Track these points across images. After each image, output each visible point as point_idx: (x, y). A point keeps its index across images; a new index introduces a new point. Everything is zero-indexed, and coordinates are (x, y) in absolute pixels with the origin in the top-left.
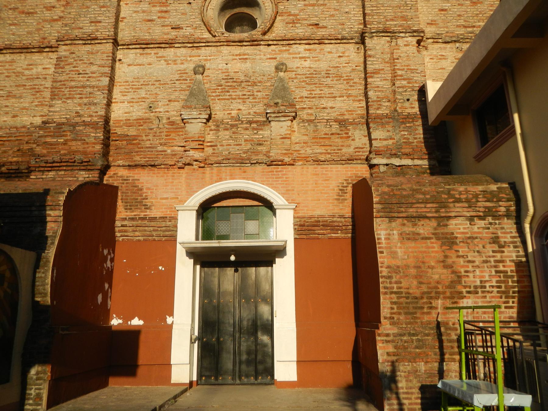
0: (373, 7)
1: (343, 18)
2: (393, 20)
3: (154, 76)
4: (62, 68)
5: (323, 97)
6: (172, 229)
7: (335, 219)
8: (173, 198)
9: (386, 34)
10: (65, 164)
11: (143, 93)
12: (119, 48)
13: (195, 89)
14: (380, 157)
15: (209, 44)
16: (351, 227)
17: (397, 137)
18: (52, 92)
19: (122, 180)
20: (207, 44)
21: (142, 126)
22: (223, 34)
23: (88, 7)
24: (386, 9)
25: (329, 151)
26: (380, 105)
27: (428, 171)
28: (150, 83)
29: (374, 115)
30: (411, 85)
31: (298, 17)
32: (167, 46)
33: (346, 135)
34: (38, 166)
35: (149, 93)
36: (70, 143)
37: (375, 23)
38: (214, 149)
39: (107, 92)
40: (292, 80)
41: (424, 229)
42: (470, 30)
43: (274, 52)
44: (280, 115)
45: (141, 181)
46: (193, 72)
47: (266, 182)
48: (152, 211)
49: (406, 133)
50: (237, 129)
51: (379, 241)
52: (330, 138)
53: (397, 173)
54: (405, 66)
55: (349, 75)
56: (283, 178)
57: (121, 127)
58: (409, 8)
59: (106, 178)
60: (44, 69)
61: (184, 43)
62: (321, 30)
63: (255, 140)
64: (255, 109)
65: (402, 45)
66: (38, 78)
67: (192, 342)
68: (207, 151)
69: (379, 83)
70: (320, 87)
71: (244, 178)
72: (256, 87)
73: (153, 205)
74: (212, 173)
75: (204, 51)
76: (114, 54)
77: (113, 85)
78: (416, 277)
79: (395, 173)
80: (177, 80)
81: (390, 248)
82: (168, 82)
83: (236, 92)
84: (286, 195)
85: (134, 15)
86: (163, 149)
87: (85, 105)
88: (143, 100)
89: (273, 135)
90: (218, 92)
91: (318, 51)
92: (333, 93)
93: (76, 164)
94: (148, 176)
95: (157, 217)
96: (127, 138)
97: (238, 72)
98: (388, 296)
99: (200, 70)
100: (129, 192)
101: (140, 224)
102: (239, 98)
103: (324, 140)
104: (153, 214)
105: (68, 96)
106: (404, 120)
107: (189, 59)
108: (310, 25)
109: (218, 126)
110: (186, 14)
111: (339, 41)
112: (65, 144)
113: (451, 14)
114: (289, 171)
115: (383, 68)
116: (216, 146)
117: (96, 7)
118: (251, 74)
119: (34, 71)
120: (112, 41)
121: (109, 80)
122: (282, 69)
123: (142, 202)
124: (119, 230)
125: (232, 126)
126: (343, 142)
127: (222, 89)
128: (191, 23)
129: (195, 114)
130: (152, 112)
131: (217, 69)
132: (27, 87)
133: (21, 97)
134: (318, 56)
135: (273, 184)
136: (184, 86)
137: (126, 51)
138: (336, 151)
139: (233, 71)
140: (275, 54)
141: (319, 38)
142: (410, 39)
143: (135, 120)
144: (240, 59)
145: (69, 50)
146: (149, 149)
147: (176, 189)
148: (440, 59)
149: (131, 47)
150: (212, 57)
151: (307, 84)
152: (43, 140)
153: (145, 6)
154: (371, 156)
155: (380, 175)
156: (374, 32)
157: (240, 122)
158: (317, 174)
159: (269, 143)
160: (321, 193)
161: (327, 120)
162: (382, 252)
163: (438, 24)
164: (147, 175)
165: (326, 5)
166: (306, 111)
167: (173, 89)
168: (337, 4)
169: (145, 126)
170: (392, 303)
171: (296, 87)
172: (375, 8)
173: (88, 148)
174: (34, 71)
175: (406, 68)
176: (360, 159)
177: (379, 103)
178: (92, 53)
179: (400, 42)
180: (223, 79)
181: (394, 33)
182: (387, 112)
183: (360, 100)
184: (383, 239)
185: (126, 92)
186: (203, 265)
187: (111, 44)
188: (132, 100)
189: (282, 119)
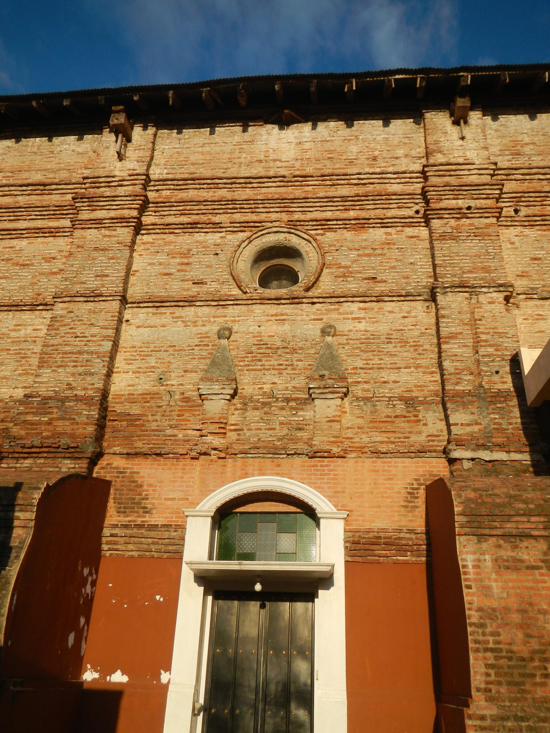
0: (445, 256)
1: (407, 270)
2: (471, 272)
3: (167, 341)
4: (56, 329)
5: (383, 368)
6: (177, 542)
7: (402, 535)
8: (183, 499)
9: (464, 290)
10: (46, 450)
11: (152, 361)
12: (127, 306)
13: (218, 356)
14: (463, 449)
15: (238, 302)
16: (425, 547)
17: (485, 422)
18: (40, 358)
19: (117, 472)
20: (236, 302)
21: (148, 402)
22: (256, 290)
23: (94, 259)
24: (463, 259)
25: (392, 439)
26: (460, 379)
27: (531, 469)
28: (162, 349)
29: (452, 392)
31: (350, 269)
32: (187, 304)
33: (415, 419)
34: (12, 451)
35: (160, 361)
36: (55, 423)
37: (449, 276)
38: (239, 435)
39: (108, 359)
40: (343, 346)
41: (529, 554)
43: (319, 312)
44: (327, 390)
45: (141, 474)
46: (216, 336)
47: (308, 481)
48: (153, 516)
49: (497, 417)
50: (270, 408)
51: (465, 570)
52: (393, 422)
53: (487, 471)
54: (490, 328)
55: (417, 340)
56: (329, 474)
57: (122, 403)
58: (492, 257)
59: (96, 469)
60: (34, 330)
61: (207, 301)
63: (293, 423)
64: (294, 383)
65: (485, 302)
66: (25, 341)
67: (195, 715)
68: (230, 437)
69: (457, 350)
70: (379, 355)
71: (277, 474)
72: (296, 355)
73: (155, 508)
74: (235, 466)
75: (232, 311)
76: (120, 313)
77: (117, 351)
78: (521, 626)
79: (484, 472)
80: (196, 346)
81: (481, 580)
83: (270, 361)
84: (334, 499)
85: (148, 268)
86: (173, 433)
87: (80, 374)
88: (153, 370)
89: (317, 417)
90: (248, 361)
91: (376, 310)
92: (396, 363)
93: (59, 450)
94: (151, 468)
95: (158, 525)
96: (128, 418)
97: (274, 336)
98: (480, 655)
100: (125, 489)
101: (135, 533)
102: (274, 369)
103: (386, 424)
104: (153, 519)
105: (59, 363)
106: (494, 400)
107: (212, 320)
108: (366, 279)
109: (245, 404)
110: (211, 267)
111: (402, 298)
112: (49, 423)
113: (547, 263)
114: (338, 466)
115: (461, 331)
116: (242, 430)
117: (104, 258)
118: (290, 338)
119: (22, 333)
120: (119, 298)
121: (112, 345)
122: (330, 332)
123: (140, 503)
124: (106, 541)
125: (264, 404)
126: (411, 427)
127: (252, 357)
128: (217, 277)
129: (216, 388)
130: (162, 386)
131: (247, 332)
132: (11, 352)
134: (375, 316)
135: (317, 483)
136: (205, 353)
137: (135, 310)
138: (402, 440)
139: (267, 334)
140: (322, 314)
141: (377, 295)
142: (495, 295)
143: (140, 394)
144: (276, 320)
145: (67, 308)
146: (155, 433)
147: (187, 486)
148: (537, 319)
149: (142, 305)
150: (242, 318)
151: (362, 351)
152: (22, 418)
153: (162, 258)
154: (450, 447)
155: (464, 473)
156: (447, 287)
157: (275, 399)
158: (376, 471)
159: (311, 427)
160: (383, 497)
161: (390, 398)
162: (469, 587)
163: (531, 276)
164: (149, 466)
165: (385, 255)
166: (360, 386)
167: (191, 357)
168: (399, 254)
169: (152, 403)
170: (487, 666)
171: (348, 356)
172: (448, 258)
173: (78, 429)
174: (22, 333)
175: (491, 331)
176: (435, 451)
177: (458, 376)
178: (94, 312)
179: (482, 298)
180: (254, 345)
181: (473, 288)
182: (469, 388)
183: (432, 373)
184: (470, 567)
185: (132, 360)
186: (217, 596)
187: (118, 302)
188: (139, 370)
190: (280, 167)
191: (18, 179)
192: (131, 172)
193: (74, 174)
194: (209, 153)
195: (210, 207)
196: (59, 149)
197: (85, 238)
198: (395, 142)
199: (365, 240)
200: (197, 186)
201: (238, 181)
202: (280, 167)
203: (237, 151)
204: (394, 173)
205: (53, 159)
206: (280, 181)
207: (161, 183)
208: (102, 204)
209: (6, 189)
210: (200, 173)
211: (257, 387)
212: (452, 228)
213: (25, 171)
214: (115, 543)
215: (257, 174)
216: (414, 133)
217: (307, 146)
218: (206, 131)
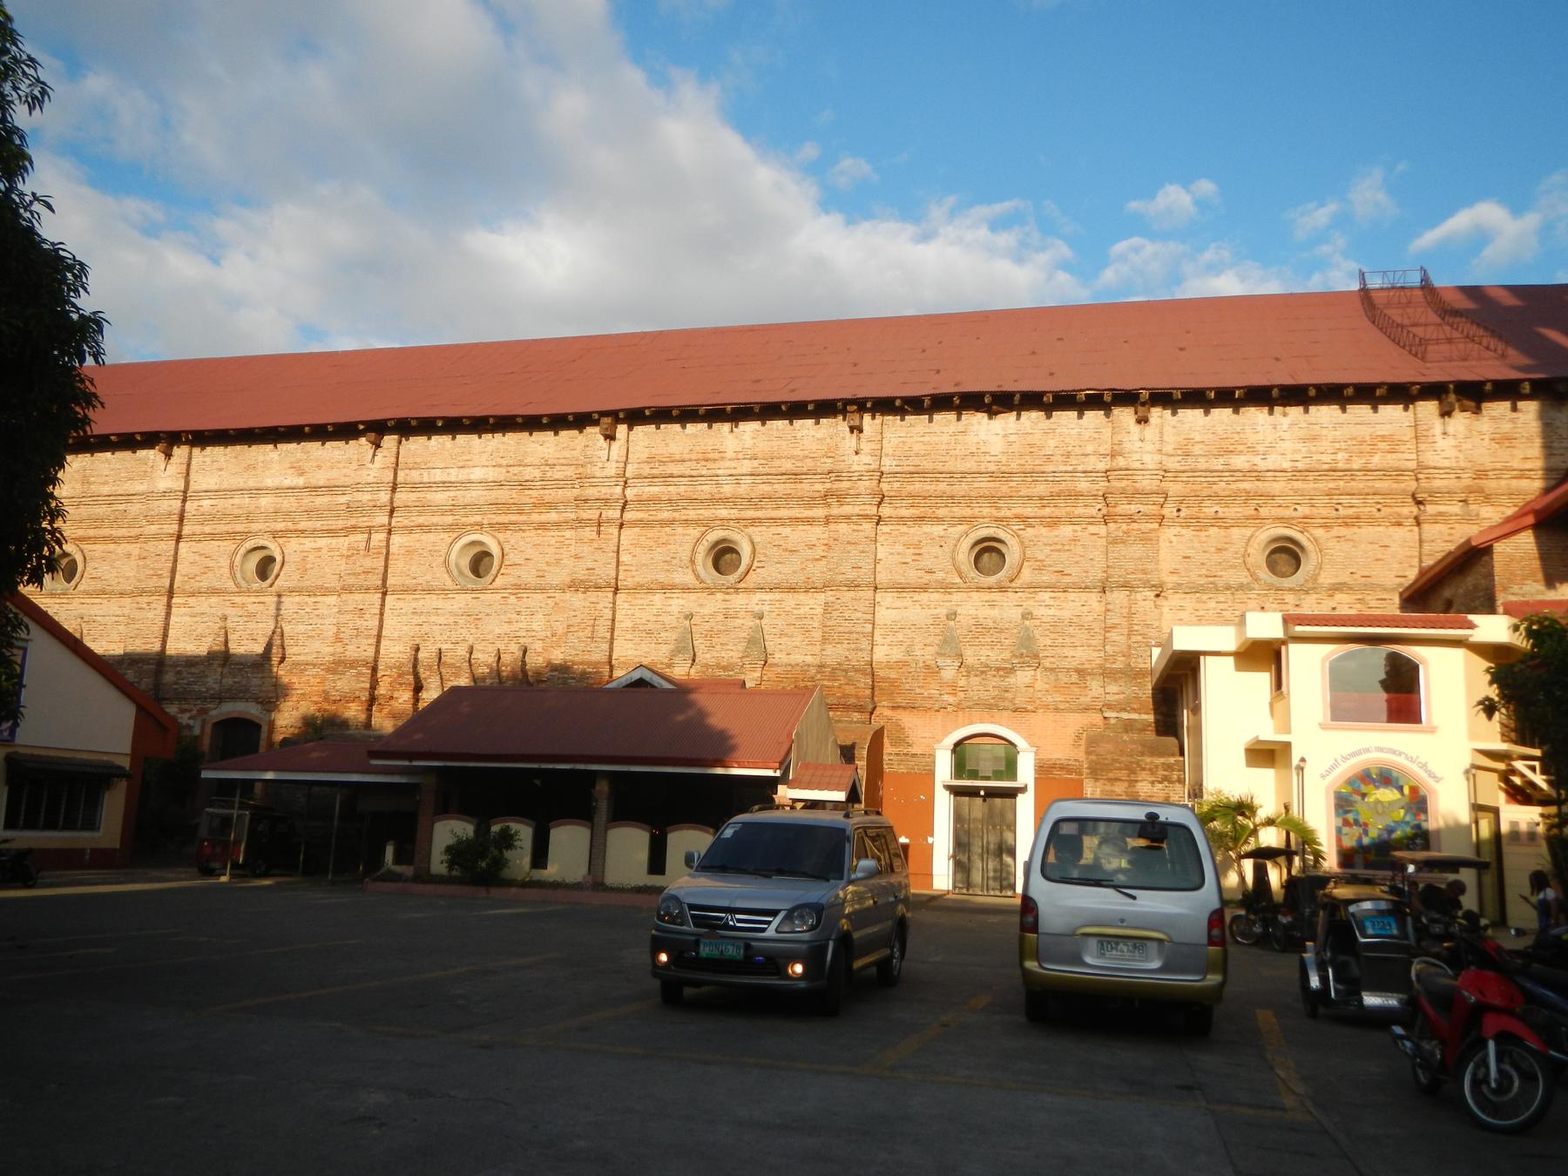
7: (1070, 763)
11: (900, 637)
21: (901, 668)
30: (1145, 640)
32: (921, 590)
42: (1211, 579)
52: (1069, 687)
62: (1066, 577)
64: (1002, 656)
67: (949, 859)
71: (992, 723)
75: (957, 597)
82: (923, 626)
85: (890, 557)
99: (952, 616)
102: (988, 645)
105: (837, 641)
107: (942, 604)
108: (1056, 572)
111: (1082, 590)
125: (982, 672)
129: (949, 661)
133: (792, 636)
136: (938, 631)
140: (1022, 601)
145: (835, 596)
149: (889, 590)
153: (899, 548)
165: (1071, 550)
174: (802, 611)
175: (1142, 623)
178: (855, 599)
179: (1139, 596)
189: (1027, 669)
193: (818, 463)
195: (933, 501)
196: (800, 434)
198: (1086, 438)
199: (1057, 536)
201: (955, 476)
204: (1084, 472)
205: (797, 445)
206: (991, 477)
207: (892, 475)
209: (765, 477)
211: (976, 658)
212: (1124, 532)
214: (892, 764)
216: (1104, 428)
217: (1012, 438)
218: (925, 418)
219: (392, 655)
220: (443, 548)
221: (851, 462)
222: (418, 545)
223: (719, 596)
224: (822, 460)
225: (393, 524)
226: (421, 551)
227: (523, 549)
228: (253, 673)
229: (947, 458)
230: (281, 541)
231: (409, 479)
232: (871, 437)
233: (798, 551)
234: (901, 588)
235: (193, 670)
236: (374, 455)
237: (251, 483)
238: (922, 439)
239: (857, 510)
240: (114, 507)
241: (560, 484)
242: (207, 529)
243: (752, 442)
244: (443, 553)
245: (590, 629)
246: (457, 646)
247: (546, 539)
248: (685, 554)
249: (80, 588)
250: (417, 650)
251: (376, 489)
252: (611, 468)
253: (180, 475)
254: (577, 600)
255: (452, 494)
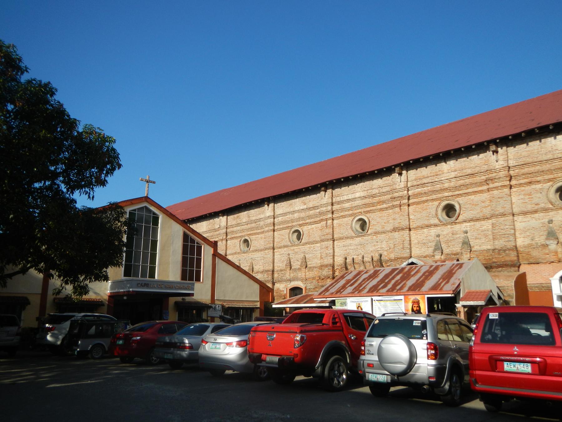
32: (534, 213)
75: (551, 213)
85: (518, 201)
107: (545, 217)
117: (502, 201)
119: (483, 228)
129: (551, 241)
136: (545, 229)
149: (519, 215)
153: (522, 197)
174: (483, 228)
190: (558, 153)
191: (463, 173)
192: (502, 166)
193: (482, 168)
194: (529, 151)
195: (534, 175)
197: (493, 194)
200: (528, 166)
201: (543, 162)
202: (558, 153)
203: (540, 148)
205: (472, 163)
208: (496, 181)
209: (460, 178)
210: (528, 161)
213: (464, 169)
215: (549, 158)
219: (339, 262)
220: (350, 222)
221: (495, 165)
222: (342, 223)
223: (449, 226)
224: (483, 167)
225: (334, 217)
226: (343, 225)
227: (376, 219)
228: (299, 272)
229: (538, 155)
230: (302, 227)
231: (337, 200)
232: (502, 153)
233: (478, 204)
234: (525, 213)
235: (282, 272)
236: (325, 194)
237: (292, 210)
238: (525, 150)
239: (500, 184)
240: (257, 223)
241: (384, 194)
242: (281, 227)
243: (453, 165)
244: (350, 224)
245: (402, 245)
246: (359, 256)
247: (383, 214)
248: (433, 213)
249: (251, 249)
250: (346, 259)
251: (327, 206)
252: (402, 185)
253: (272, 211)
254: (396, 235)
255: (350, 203)
